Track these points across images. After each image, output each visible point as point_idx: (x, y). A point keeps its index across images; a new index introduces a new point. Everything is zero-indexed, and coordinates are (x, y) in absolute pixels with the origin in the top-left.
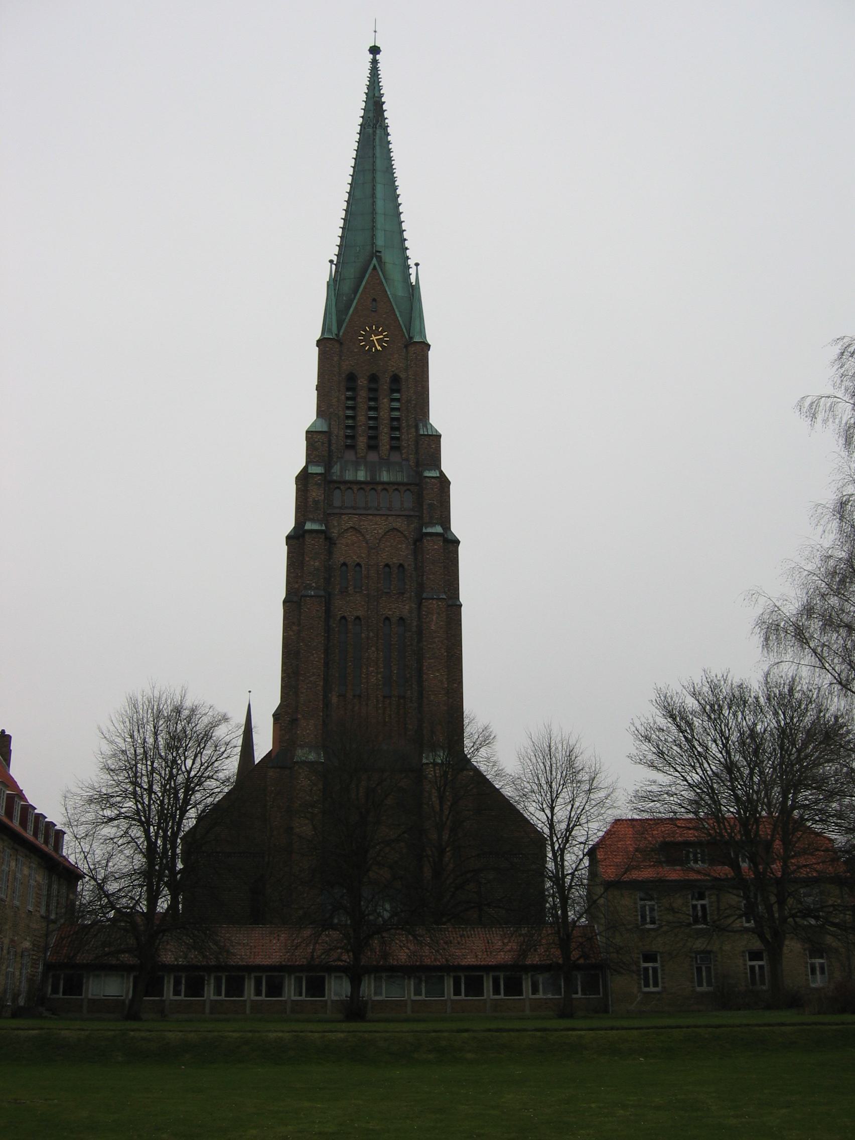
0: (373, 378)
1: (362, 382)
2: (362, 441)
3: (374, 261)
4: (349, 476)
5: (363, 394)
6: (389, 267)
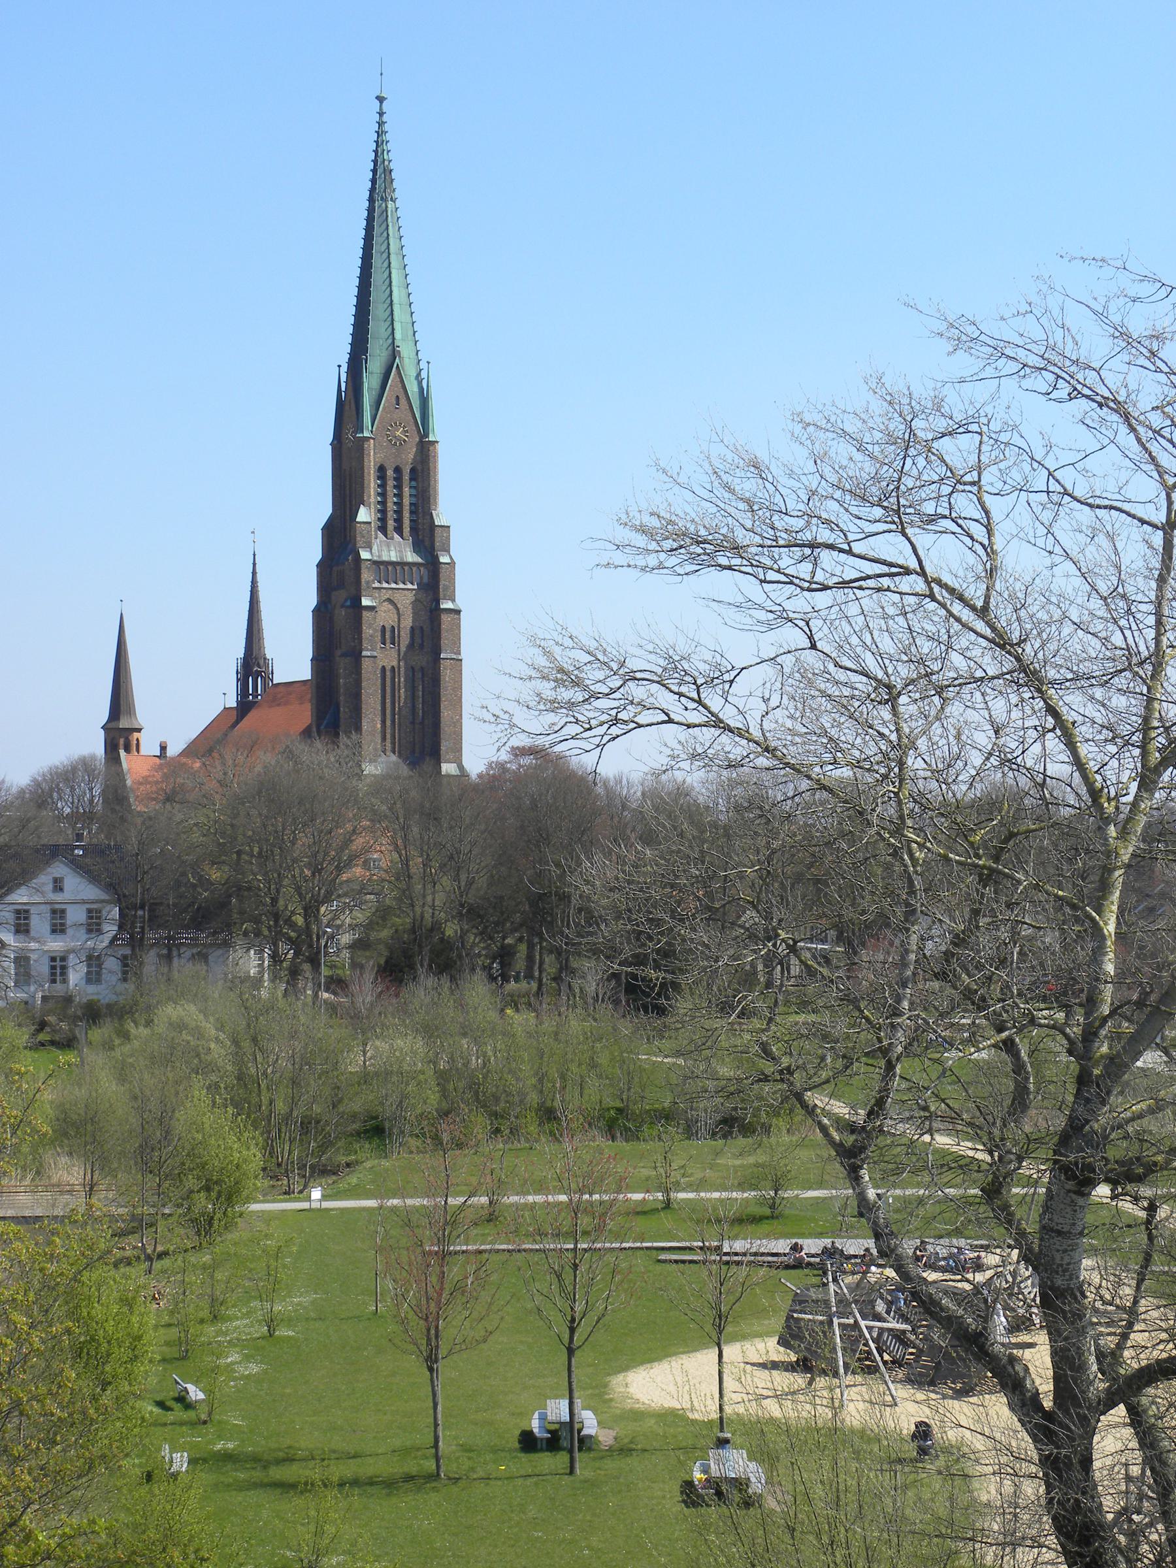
0: (398, 470)
1: (390, 473)
2: (391, 524)
3: (397, 360)
4: (385, 558)
5: (391, 483)
6: (406, 361)
